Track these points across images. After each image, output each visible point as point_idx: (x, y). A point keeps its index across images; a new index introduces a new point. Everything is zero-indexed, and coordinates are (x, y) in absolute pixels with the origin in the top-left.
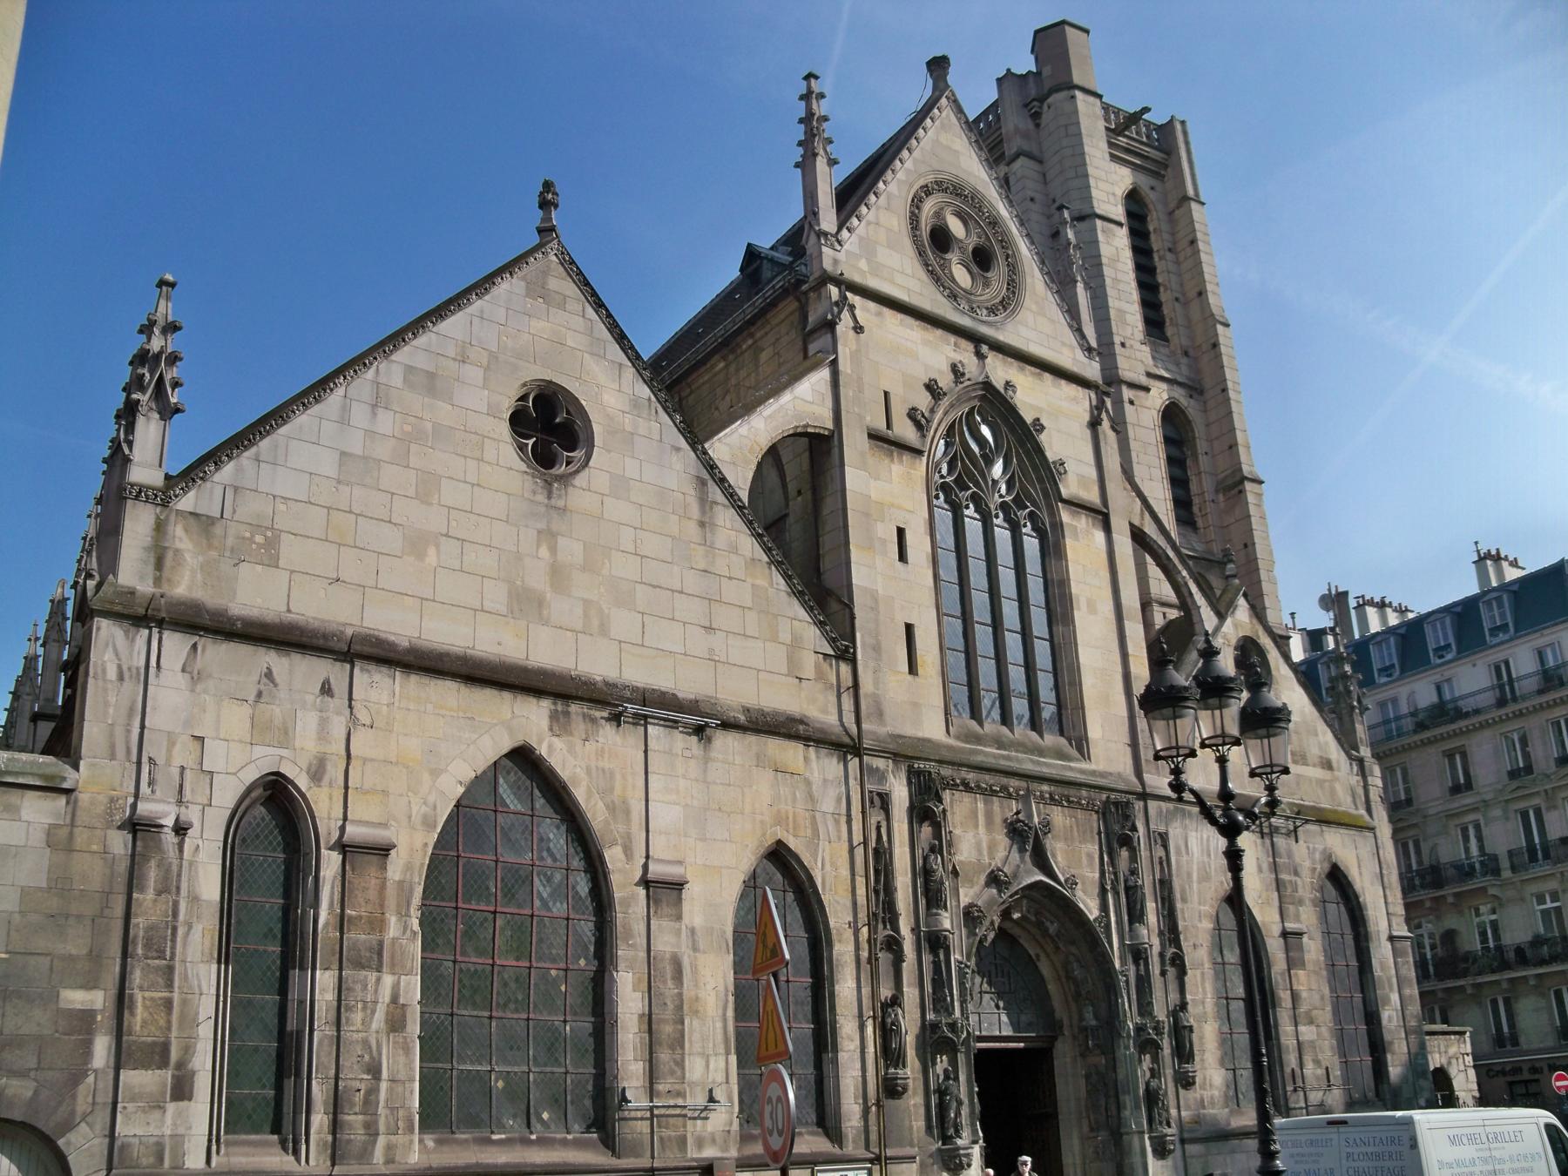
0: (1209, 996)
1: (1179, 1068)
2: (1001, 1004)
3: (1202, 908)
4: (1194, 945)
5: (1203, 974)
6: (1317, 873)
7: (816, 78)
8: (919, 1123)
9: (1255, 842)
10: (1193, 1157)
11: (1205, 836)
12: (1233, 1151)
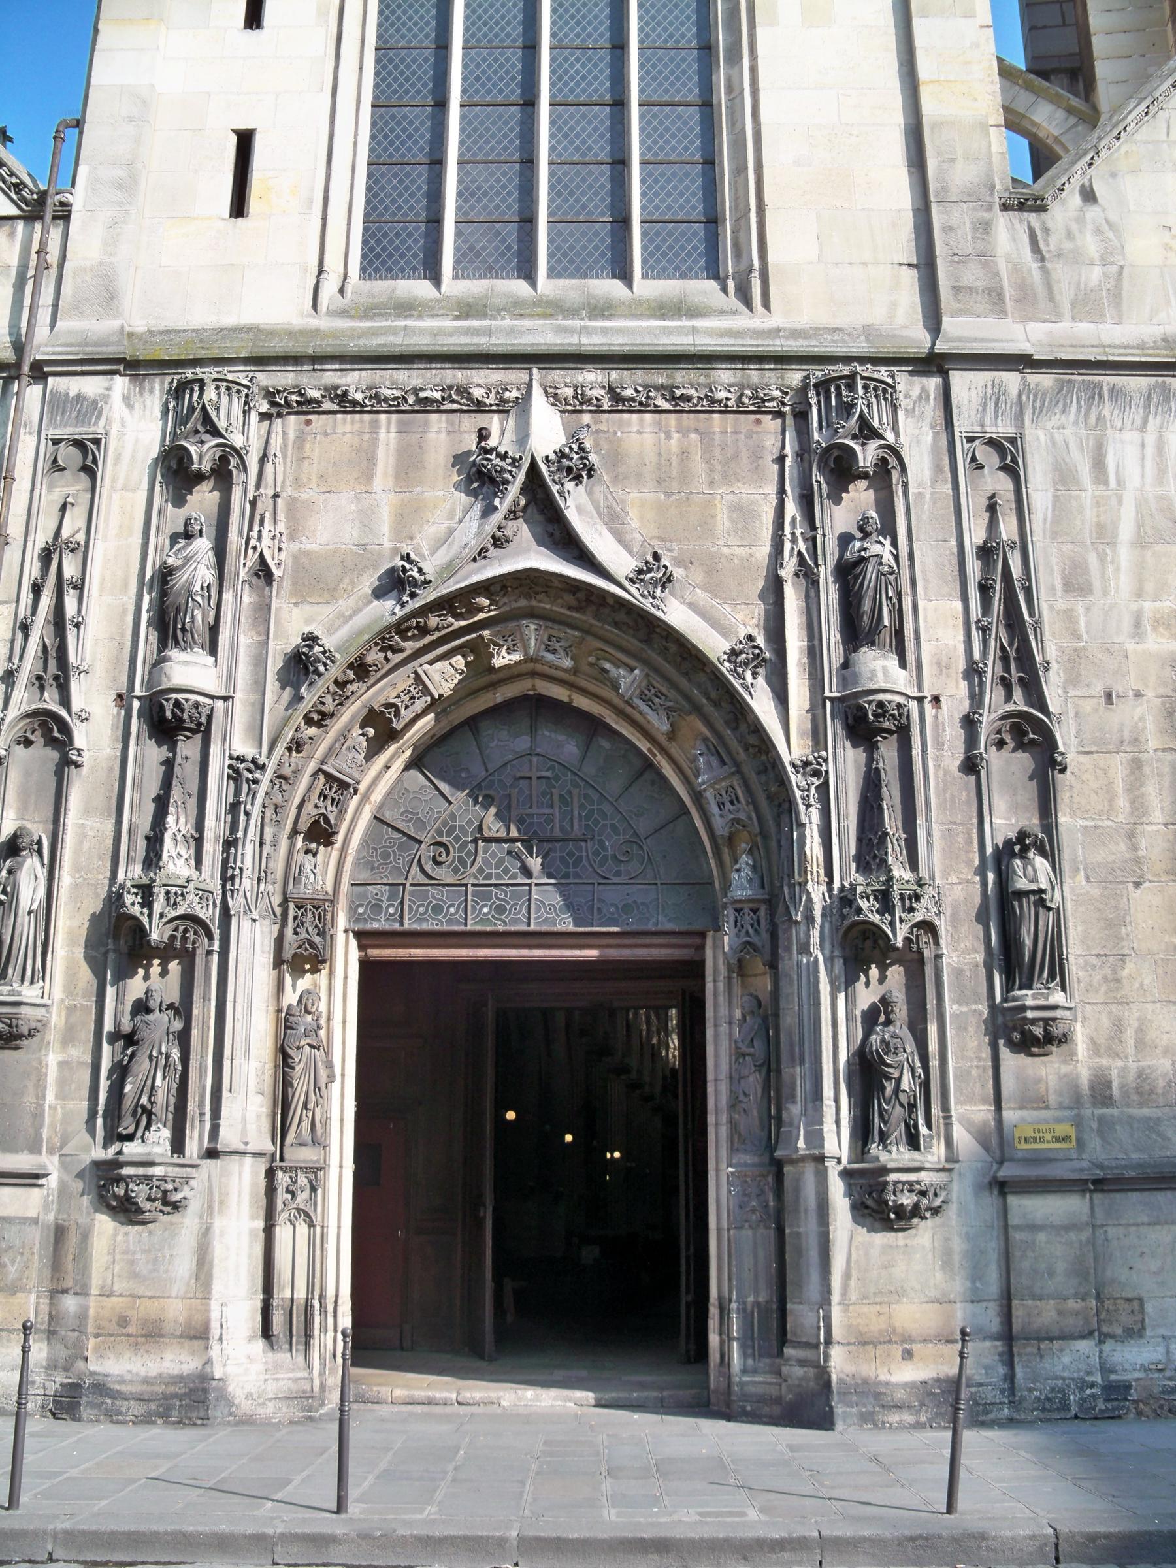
0: (1157, 816)
1: (1005, 1000)
2: (535, 863)
3: (1147, 605)
4: (1109, 696)
5: (1136, 765)
8: (71, 1104)
10: (1034, 1228)
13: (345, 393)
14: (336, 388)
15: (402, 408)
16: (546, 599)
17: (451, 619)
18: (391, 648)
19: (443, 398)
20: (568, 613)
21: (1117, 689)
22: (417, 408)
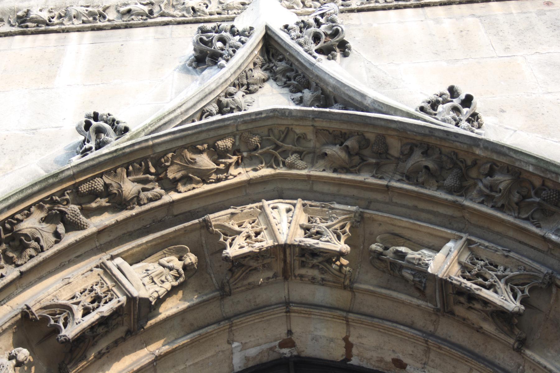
13: (28, 12)
14: (19, 10)
15: (99, 24)
16: (300, 163)
17: (158, 190)
18: (62, 217)
19: (151, 12)
20: (335, 175)
22: (119, 22)
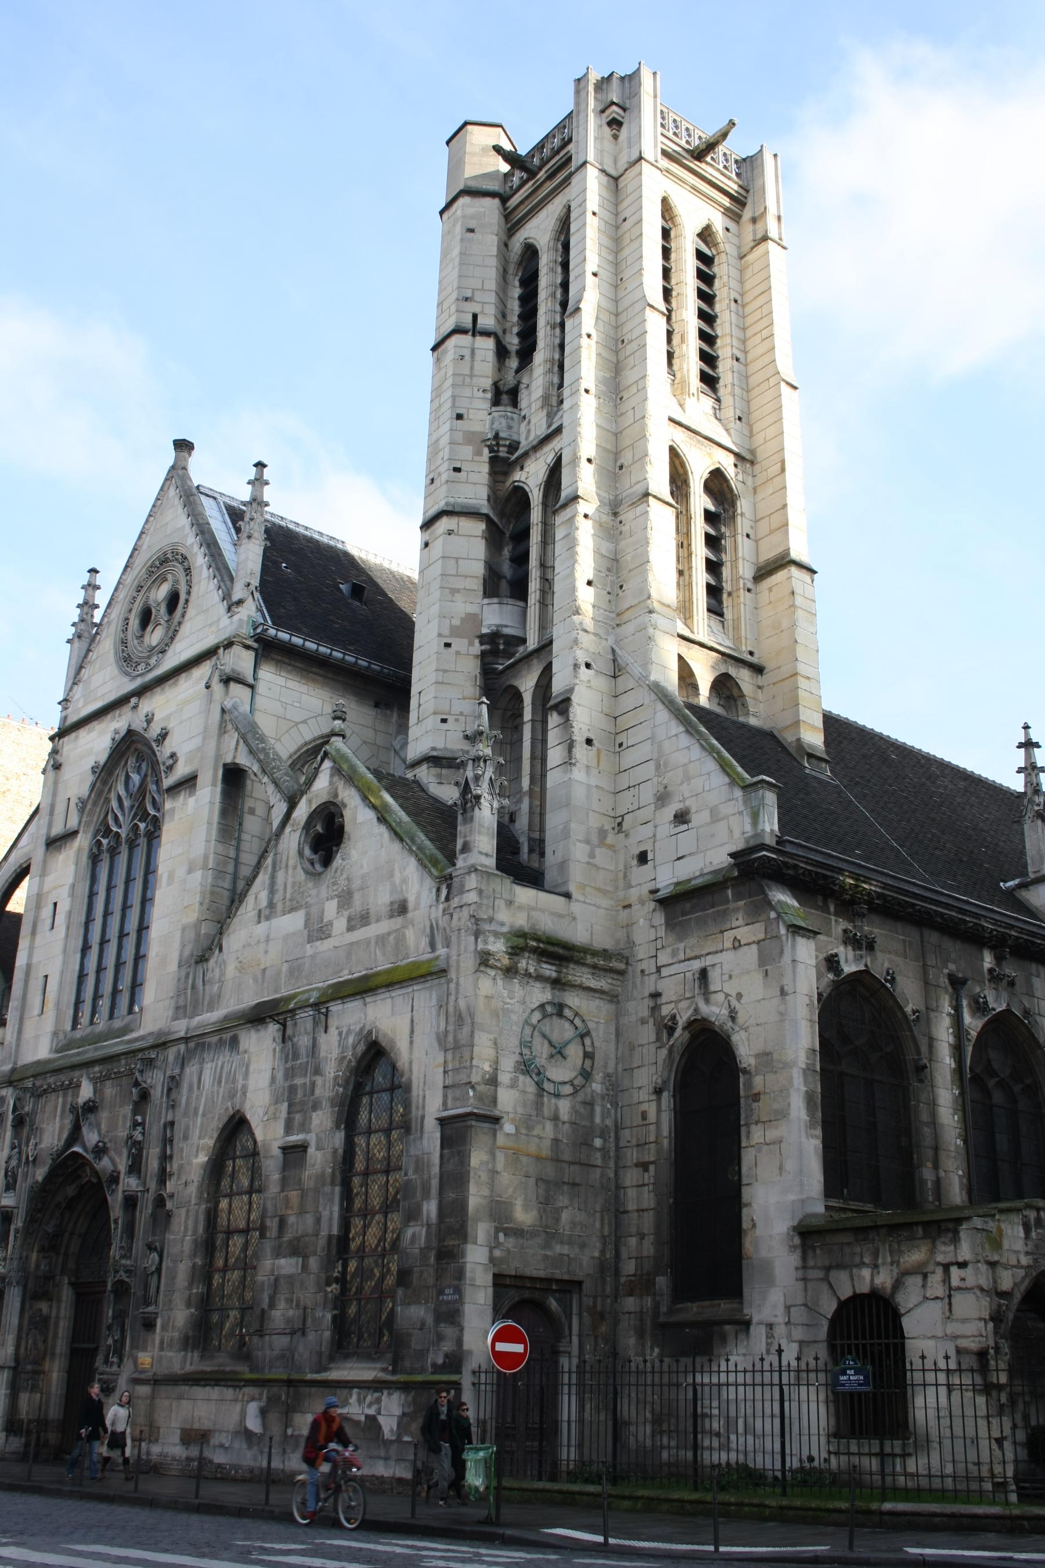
0: (190, 1233)
5: (188, 1211)
6: (345, 1063)
7: (265, 466)
9: (274, 1050)
10: (138, 1398)
11: (220, 1063)
12: (180, 1398)
21: (189, 1180)
